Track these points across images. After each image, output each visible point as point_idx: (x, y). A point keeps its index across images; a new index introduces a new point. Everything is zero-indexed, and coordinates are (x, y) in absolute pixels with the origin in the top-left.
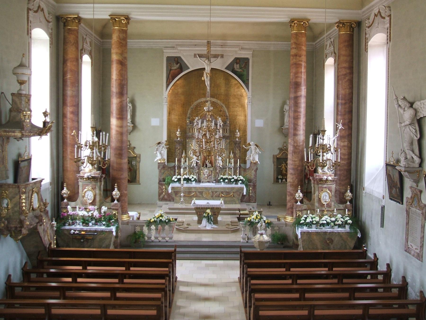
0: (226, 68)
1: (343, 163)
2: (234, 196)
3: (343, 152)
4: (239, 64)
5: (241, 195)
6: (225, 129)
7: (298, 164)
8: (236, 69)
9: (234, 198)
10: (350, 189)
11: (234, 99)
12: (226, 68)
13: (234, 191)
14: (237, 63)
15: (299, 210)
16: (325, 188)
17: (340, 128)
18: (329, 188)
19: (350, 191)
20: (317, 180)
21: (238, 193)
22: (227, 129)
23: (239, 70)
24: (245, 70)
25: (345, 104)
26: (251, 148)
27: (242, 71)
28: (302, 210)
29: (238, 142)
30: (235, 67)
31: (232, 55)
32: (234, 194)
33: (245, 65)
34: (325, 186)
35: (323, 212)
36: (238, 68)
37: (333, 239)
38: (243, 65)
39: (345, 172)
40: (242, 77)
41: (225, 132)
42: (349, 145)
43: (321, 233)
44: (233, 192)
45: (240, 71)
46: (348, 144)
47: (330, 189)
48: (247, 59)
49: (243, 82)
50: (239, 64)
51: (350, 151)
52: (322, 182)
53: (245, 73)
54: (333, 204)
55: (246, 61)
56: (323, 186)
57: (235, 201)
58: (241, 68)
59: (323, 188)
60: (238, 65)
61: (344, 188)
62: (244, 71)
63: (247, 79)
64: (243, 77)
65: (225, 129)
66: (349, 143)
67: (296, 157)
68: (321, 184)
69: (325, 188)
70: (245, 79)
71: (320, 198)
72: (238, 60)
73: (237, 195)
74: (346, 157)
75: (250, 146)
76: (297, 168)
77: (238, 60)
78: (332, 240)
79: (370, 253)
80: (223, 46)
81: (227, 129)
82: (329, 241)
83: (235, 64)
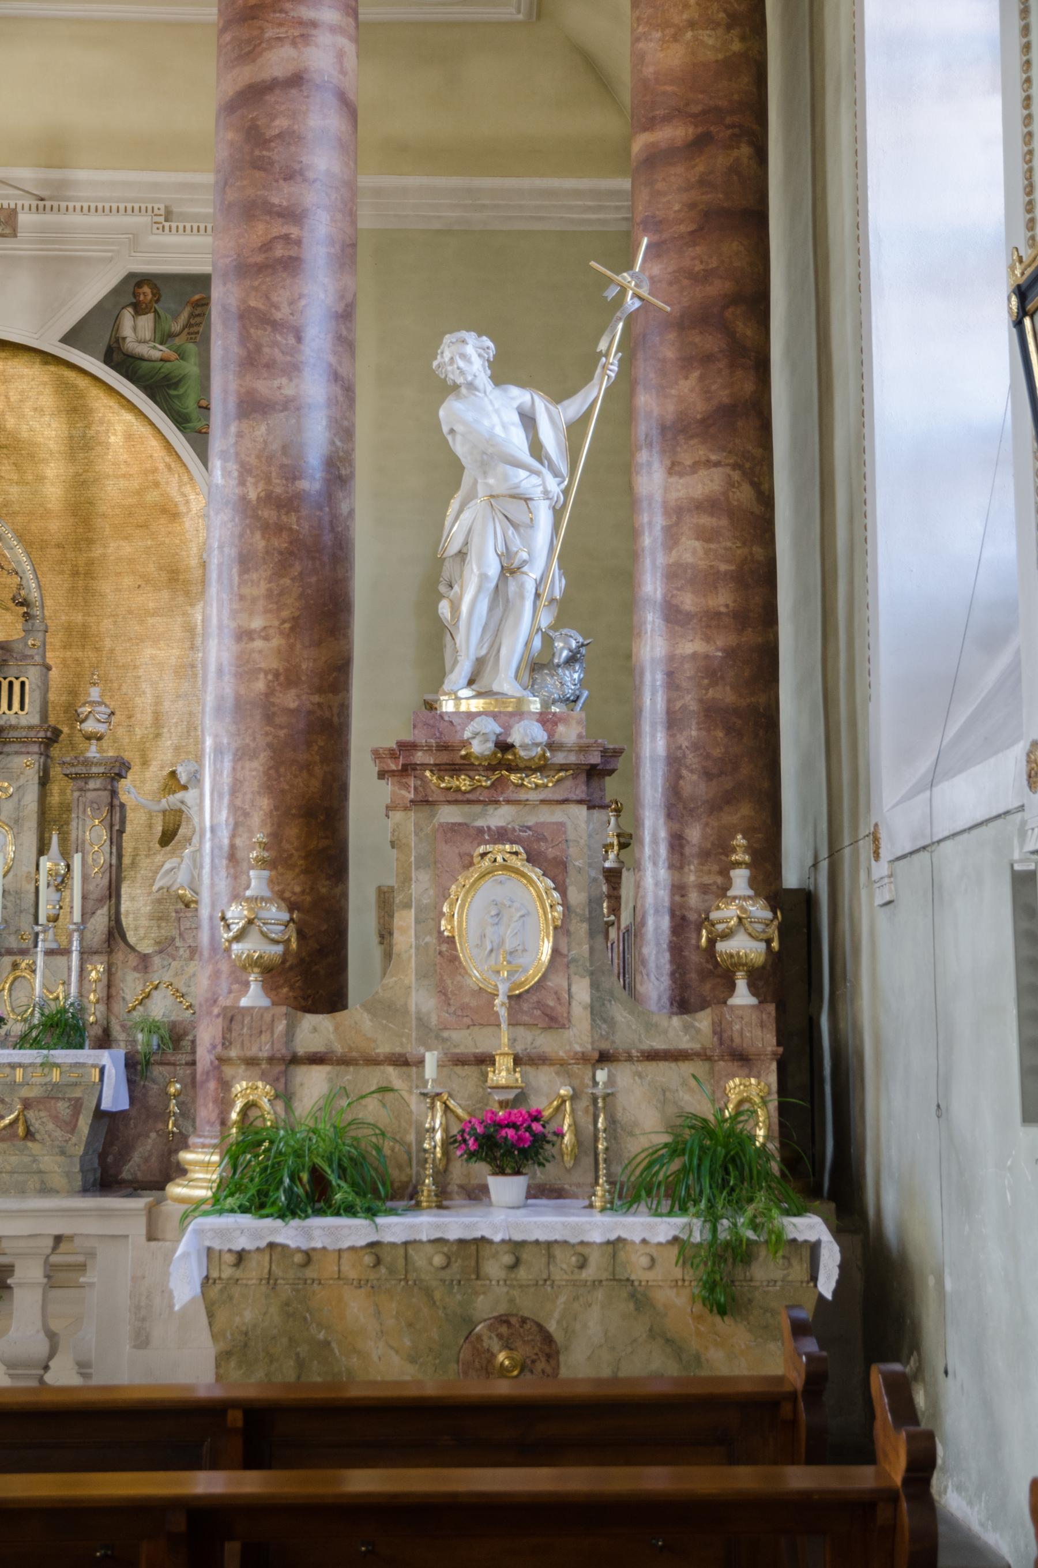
0: (68, 339)
1: (694, 656)
2: (29, 1135)
3: (688, 558)
4: (151, 316)
5: (84, 1124)
6: (11, 684)
7: (275, 665)
8: (132, 345)
9: (30, 1144)
10: (748, 866)
11: (126, 538)
12: (68, 339)
13: (25, 1092)
14: (139, 309)
15: (251, 1062)
16: (501, 836)
17: (632, 304)
18: (541, 838)
19: (752, 883)
20: (419, 757)
21: (63, 1108)
22: (23, 684)
23: (153, 352)
24: (191, 348)
25: (699, 144)
26: (182, 802)
27: (173, 356)
28: (295, 1060)
29: (98, 764)
30: (127, 329)
31: (111, 259)
32: (31, 1114)
33: (192, 315)
34: (498, 817)
35: (485, 1076)
36: (148, 334)
37: (552, 1327)
38: (175, 317)
39: (720, 734)
40: (173, 392)
41: (10, 707)
42: (744, 495)
43: (419, 1259)
44: (27, 1104)
45: (156, 354)
46: (731, 484)
47: (551, 853)
48: (202, 282)
49: (180, 420)
50: (151, 316)
51: (758, 551)
52: (463, 783)
53: (191, 368)
54: (582, 992)
55: (197, 297)
56: (480, 823)
57: (40, 1172)
58: (164, 337)
59: (480, 835)
60: (146, 322)
61: (707, 880)
62: (182, 356)
63: (203, 403)
64: (181, 391)
65: (11, 684)
66: (736, 475)
67: (254, 600)
68: (457, 798)
69: (501, 836)
70: (190, 405)
71: (451, 940)
72: (146, 289)
73: (51, 1126)
74: (723, 599)
75: (180, 795)
76: (270, 693)
77: (146, 289)
78: (548, 1338)
79: (959, 1488)
80: (48, 204)
81: (23, 684)
82: (508, 1346)
83: (128, 315)
